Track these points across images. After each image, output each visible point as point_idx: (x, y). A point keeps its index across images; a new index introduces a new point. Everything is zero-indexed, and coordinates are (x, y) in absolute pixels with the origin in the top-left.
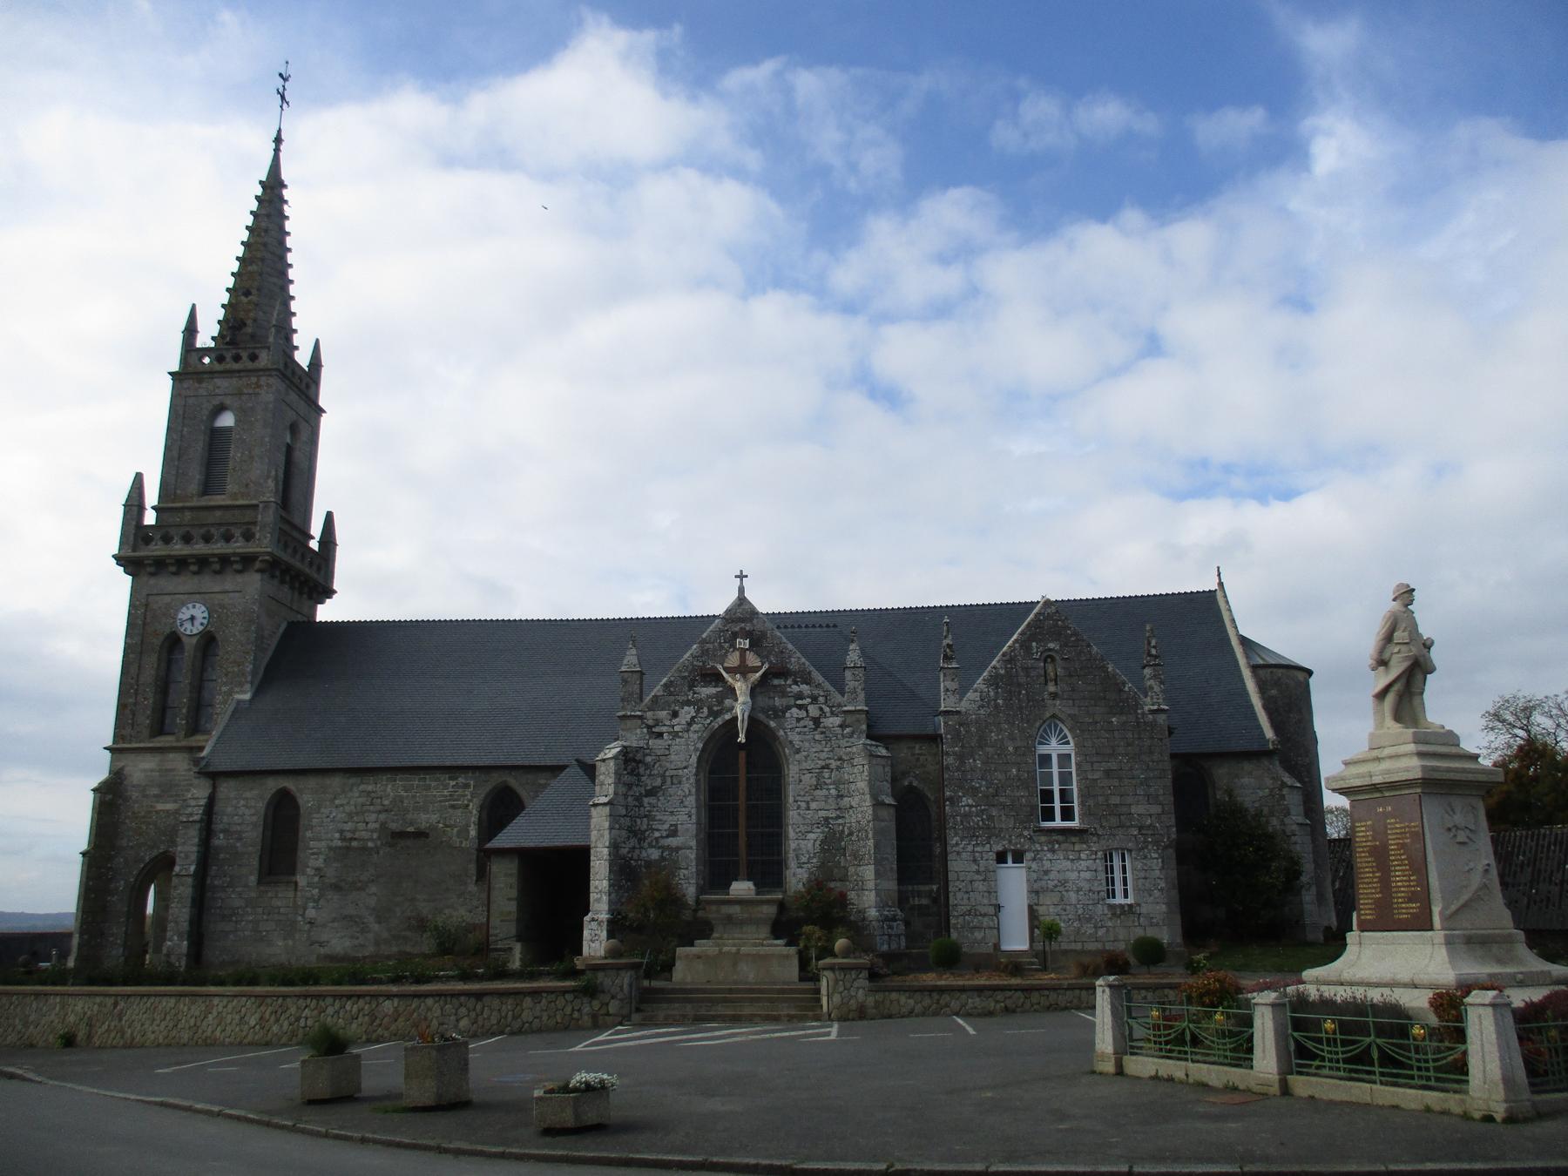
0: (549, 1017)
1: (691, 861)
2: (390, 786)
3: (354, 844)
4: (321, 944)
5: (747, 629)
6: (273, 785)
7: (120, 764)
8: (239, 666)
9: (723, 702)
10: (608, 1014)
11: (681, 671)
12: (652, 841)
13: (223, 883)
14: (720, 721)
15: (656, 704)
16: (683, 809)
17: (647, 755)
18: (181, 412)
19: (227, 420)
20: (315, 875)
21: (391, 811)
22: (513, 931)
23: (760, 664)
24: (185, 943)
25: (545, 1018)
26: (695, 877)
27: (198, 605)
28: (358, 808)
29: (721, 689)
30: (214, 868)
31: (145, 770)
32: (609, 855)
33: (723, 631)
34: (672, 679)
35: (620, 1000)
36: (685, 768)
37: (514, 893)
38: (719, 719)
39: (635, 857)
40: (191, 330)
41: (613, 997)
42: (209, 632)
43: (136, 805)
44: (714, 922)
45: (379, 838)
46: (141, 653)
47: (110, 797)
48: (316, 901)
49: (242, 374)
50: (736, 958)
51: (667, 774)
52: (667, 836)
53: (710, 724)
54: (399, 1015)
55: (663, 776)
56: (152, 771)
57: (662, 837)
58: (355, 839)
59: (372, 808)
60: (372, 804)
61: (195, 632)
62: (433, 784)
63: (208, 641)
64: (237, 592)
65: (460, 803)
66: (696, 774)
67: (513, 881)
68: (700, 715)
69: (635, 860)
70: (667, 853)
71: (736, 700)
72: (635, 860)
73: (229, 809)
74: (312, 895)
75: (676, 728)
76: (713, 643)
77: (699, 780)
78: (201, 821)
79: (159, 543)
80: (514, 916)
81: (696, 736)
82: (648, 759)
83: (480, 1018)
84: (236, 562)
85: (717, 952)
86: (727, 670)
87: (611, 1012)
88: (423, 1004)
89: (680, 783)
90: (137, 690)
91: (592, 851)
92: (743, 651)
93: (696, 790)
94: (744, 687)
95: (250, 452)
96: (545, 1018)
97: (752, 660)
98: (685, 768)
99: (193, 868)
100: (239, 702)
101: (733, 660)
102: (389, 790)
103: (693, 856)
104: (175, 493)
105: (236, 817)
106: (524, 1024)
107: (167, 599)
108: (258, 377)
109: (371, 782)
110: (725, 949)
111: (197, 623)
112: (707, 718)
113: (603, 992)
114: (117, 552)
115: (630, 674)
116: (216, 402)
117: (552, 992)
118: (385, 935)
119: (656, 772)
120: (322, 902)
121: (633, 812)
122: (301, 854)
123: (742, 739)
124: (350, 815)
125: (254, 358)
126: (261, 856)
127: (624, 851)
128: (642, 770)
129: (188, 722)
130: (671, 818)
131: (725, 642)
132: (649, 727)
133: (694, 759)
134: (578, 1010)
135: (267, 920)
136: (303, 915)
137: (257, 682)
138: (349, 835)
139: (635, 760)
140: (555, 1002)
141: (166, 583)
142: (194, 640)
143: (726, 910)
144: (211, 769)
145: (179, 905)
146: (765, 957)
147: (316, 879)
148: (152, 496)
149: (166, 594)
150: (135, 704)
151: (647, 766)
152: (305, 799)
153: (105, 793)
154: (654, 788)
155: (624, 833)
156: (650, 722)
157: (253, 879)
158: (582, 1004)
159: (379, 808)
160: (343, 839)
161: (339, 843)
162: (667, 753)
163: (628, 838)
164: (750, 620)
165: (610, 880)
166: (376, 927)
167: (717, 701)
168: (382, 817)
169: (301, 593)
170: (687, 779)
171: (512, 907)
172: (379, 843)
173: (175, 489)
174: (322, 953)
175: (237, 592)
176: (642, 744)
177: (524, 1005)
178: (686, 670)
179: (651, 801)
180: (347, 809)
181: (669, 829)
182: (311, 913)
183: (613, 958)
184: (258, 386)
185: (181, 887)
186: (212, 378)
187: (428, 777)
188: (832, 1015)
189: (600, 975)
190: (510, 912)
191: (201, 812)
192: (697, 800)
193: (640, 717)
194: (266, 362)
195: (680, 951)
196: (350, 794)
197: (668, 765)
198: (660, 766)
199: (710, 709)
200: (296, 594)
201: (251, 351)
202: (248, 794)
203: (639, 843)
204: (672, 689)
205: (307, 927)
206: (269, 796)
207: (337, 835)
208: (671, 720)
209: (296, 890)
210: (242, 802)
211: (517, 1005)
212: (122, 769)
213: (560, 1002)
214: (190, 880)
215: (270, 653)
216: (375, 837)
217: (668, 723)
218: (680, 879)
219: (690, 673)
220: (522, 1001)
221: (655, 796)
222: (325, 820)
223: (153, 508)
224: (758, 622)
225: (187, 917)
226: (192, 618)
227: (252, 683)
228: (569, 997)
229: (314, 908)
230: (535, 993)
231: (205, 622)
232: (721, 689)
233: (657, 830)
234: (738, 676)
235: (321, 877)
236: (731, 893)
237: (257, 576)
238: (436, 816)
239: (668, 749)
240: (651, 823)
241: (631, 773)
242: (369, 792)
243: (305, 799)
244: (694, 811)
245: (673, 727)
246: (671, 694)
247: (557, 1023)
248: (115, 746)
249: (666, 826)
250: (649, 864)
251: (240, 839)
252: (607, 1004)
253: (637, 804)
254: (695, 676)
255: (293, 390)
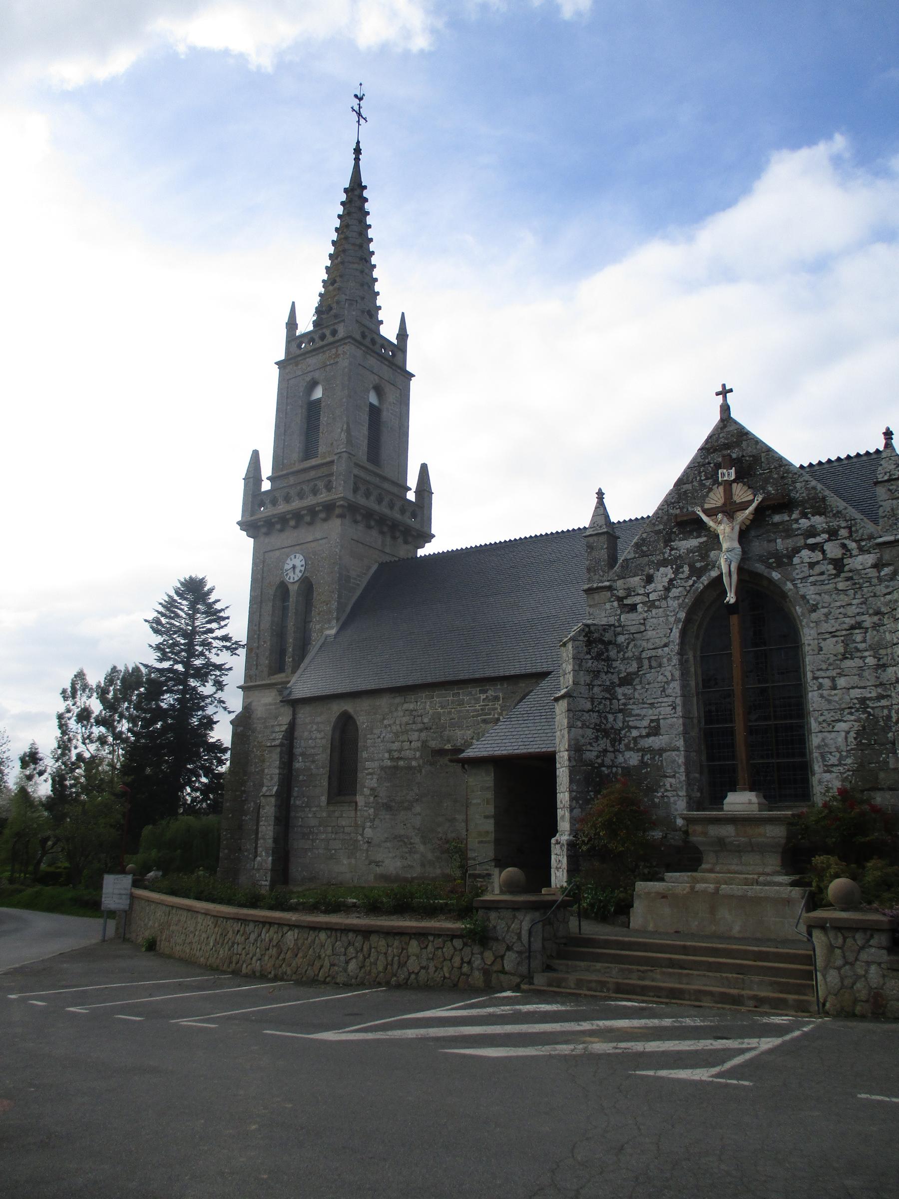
0: (437, 968)
1: (679, 766)
2: (428, 703)
3: (401, 763)
4: (378, 864)
5: (734, 456)
6: (337, 708)
7: (249, 700)
8: (327, 604)
9: (708, 556)
10: (503, 971)
11: (654, 524)
12: (630, 741)
13: (303, 803)
14: (705, 580)
15: (627, 570)
16: (665, 700)
17: (619, 634)
18: (285, 394)
19: (318, 393)
20: (371, 795)
21: (431, 729)
22: (491, 854)
23: (751, 497)
24: (270, 858)
25: (432, 969)
26: (684, 787)
27: (298, 555)
28: (403, 727)
29: (704, 539)
30: (296, 789)
31: (266, 705)
32: (569, 760)
33: (704, 465)
34: (644, 535)
35: (517, 952)
36: (666, 645)
37: (491, 810)
38: (704, 578)
39: (608, 761)
40: (292, 324)
41: (509, 948)
42: (306, 577)
43: (260, 736)
44: (701, 848)
45: (421, 757)
46: (261, 602)
47: (242, 728)
48: (372, 821)
49: (325, 349)
50: (714, 899)
51: (644, 655)
52: (648, 735)
53: (693, 585)
54: (299, 949)
55: (639, 659)
56: (270, 704)
57: (641, 736)
58: (401, 758)
59: (414, 727)
60: (414, 723)
61: (296, 579)
62: (466, 698)
63: (307, 586)
64: (324, 538)
65: (491, 716)
66: (681, 653)
67: (490, 795)
68: (681, 576)
69: (608, 767)
70: (648, 756)
71: (720, 549)
72: (608, 767)
73: (306, 734)
74: (369, 814)
75: (653, 597)
76: (692, 482)
77: (687, 661)
78: (281, 745)
79: (269, 506)
80: (491, 837)
81: (675, 604)
82: (621, 639)
83: (367, 963)
84: (320, 511)
85: (687, 890)
86: (710, 513)
87: (507, 968)
88: (317, 938)
89: (660, 666)
90: (259, 635)
91: (557, 757)
92: (728, 485)
93: (682, 674)
94: (728, 529)
95: (333, 415)
96: (432, 969)
97: (741, 493)
98: (666, 645)
99: (275, 789)
100: (327, 636)
101: (716, 498)
102: (428, 707)
103: (681, 760)
104: (283, 462)
105: (310, 741)
106: (410, 974)
107: (277, 553)
108: (337, 347)
109: (413, 700)
110: (700, 886)
111: (297, 571)
112: (688, 578)
113: (497, 939)
114: (240, 519)
115: (595, 538)
116: (308, 378)
117: (439, 936)
118: (430, 856)
119: (629, 654)
120: (377, 822)
121: (601, 707)
122: (360, 775)
123: (731, 598)
124: (397, 734)
125: (334, 333)
126: (330, 778)
127: (590, 755)
128: (613, 653)
129: (293, 660)
130: (650, 712)
131: (707, 479)
132: (620, 599)
133: (676, 633)
134: (469, 963)
135: (335, 839)
136: (362, 835)
137: (343, 617)
138: (396, 755)
139: (602, 641)
140: (442, 948)
141: (279, 540)
142: (296, 587)
143: (714, 831)
144: (293, 697)
145: (266, 823)
146: (757, 901)
147: (372, 799)
148: (267, 469)
149: (276, 550)
150: (258, 648)
151: (620, 648)
152: (361, 721)
153: (237, 726)
154: (629, 674)
155: (589, 732)
156: (621, 593)
157: (324, 799)
158: (473, 954)
159: (420, 726)
160: (391, 759)
161: (389, 763)
162: (642, 628)
163: (597, 738)
164: (738, 444)
165: (571, 791)
166: (422, 848)
167: (700, 555)
168: (423, 735)
169: (394, 538)
170: (669, 660)
171: (489, 826)
172: (421, 762)
173: (283, 459)
174: (378, 872)
175: (324, 538)
176: (612, 620)
177: (410, 950)
178: (660, 523)
179: (626, 691)
180: (395, 728)
181: (649, 727)
182: (368, 832)
183: (512, 893)
184: (337, 356)
185: (267, 807)
186: (305, 359)
187: (460, 691)
188: (828, 1005)
189: (493, 915)
190: (487, 832)
191: (281, 737)
192: (684, 687)
193: (610, 588)
194: (343, 334)
195: (640, 886)
196: (395, 714)
197: (644, 644)
198: (635, 645)
199: (692, 567)
200: (388, 539)
201: (332, 328)
202: (318, 719)
203: (613, 746)
204: (645, 548)
205: (365, 846)
206: (334, 720)
207: (387, 755)
208: (644, 587)
209: (356, 809)
210: (315, 727)
211: (403, 949)
212: (250, 704)
213: (448, 950)
214: (273, 800)
215: (358, 593)
216: (417, 756)
217: (641, 591)
218: (667, 791)
219: (665, 524)
220: (408, 944)
221: (631, 685)
222: (376, 740)
223: (268, 478)
224: (748, 445)
225: (271, 834)
226: (294, 567)
227: (338, 619)
228: (458, 943)
229: (370, 827)
230: (421, 935)
231: (303, 569)
232: (704, 539)
233: (636, 728)
234: (720, 516)
235: (376, 796)
236: (725, 807)
237: (338, 522)
238: (469, 732)
239: (644, 624)
240: (627, 719)
241: (598, 657)
242: (412, 711)
243: (361, 721)
244: (679, 701)
245: (648, 595)
246: (644, 554)
247: (445, 978)
248: (245, 685)
249: (645, 723)
250: (627, 771)
251: (313, 762)
252: (502, 957)
253: (608, 696)
254: (671, 529)
255: (373, 357)
